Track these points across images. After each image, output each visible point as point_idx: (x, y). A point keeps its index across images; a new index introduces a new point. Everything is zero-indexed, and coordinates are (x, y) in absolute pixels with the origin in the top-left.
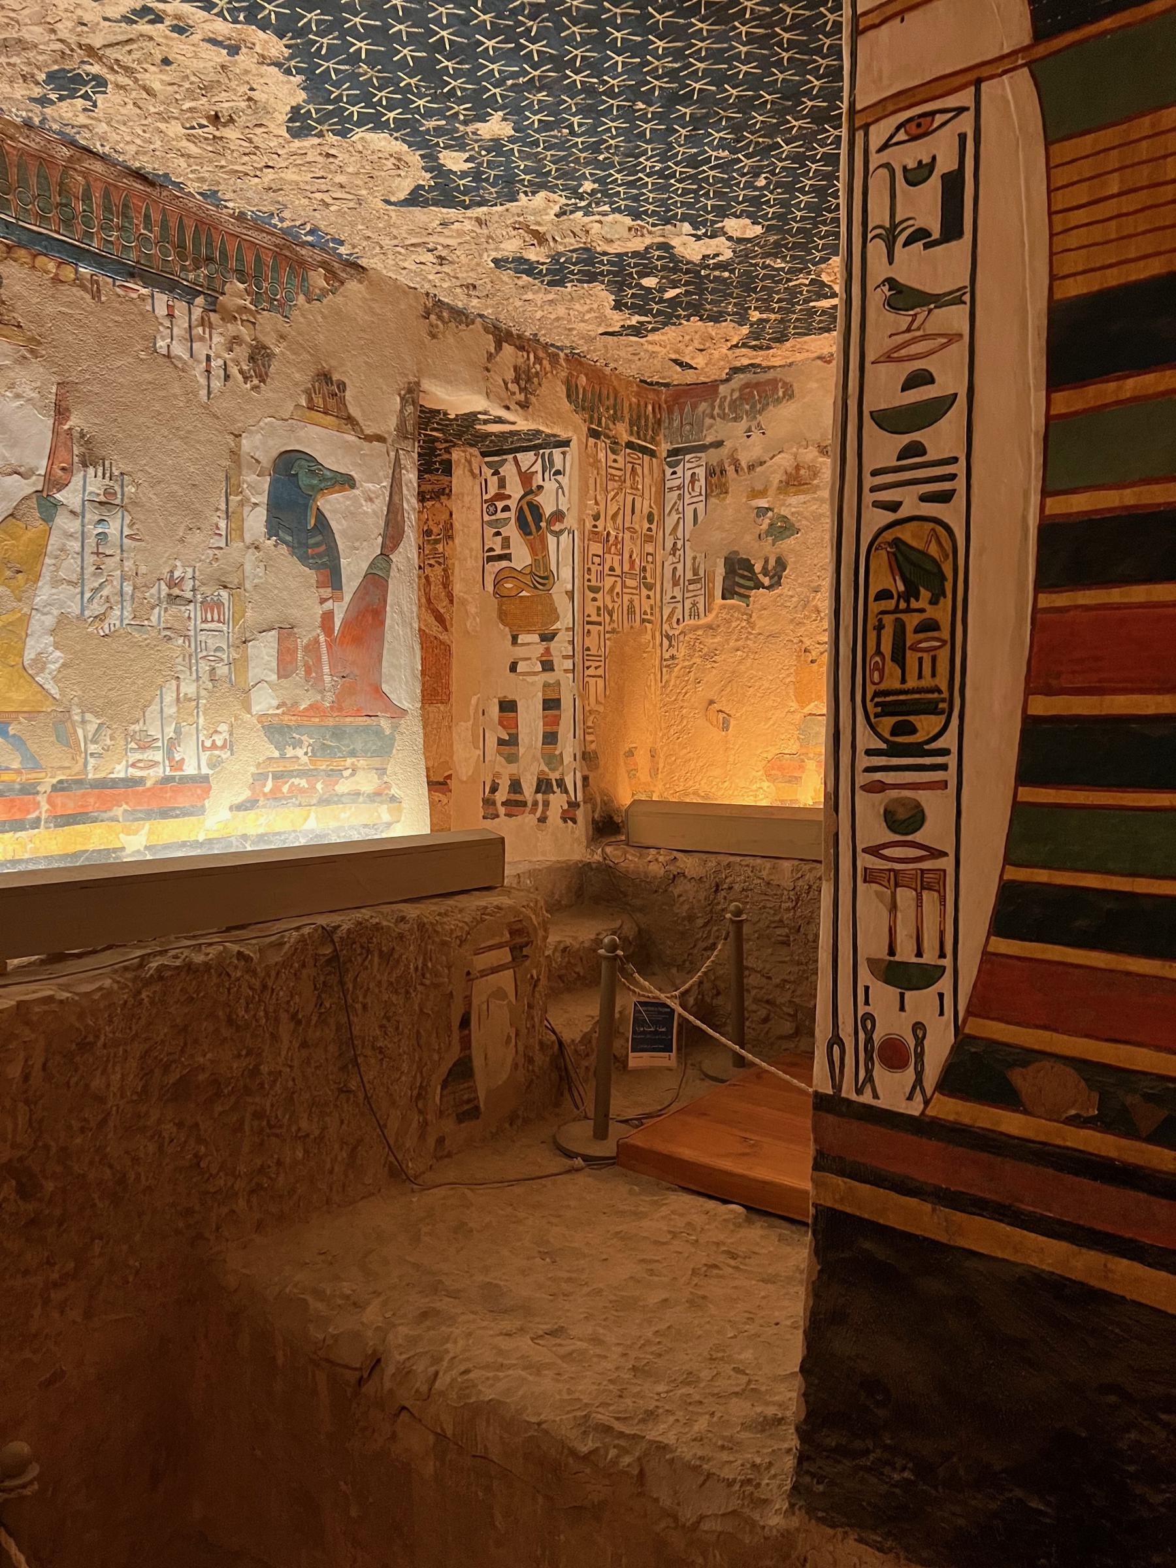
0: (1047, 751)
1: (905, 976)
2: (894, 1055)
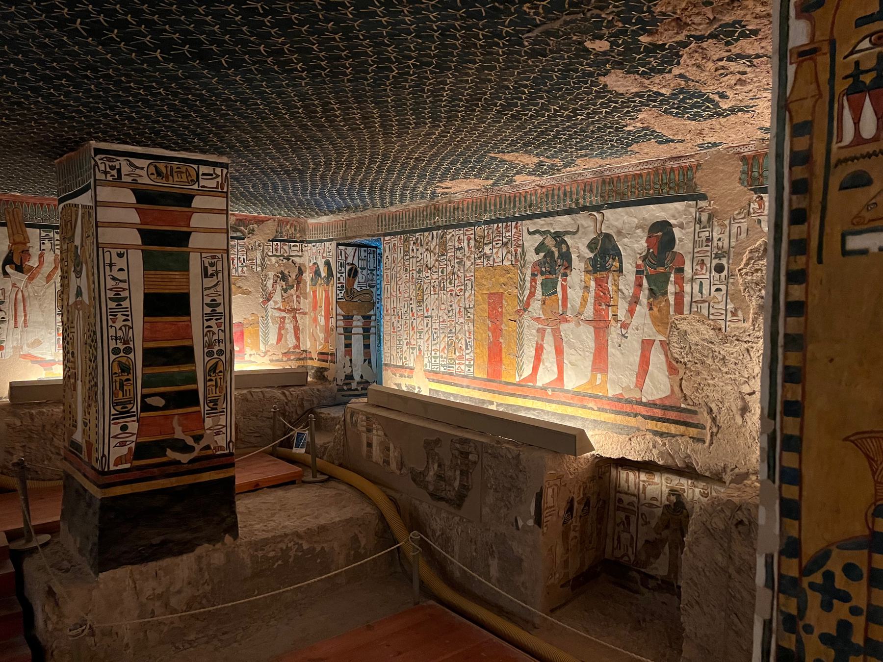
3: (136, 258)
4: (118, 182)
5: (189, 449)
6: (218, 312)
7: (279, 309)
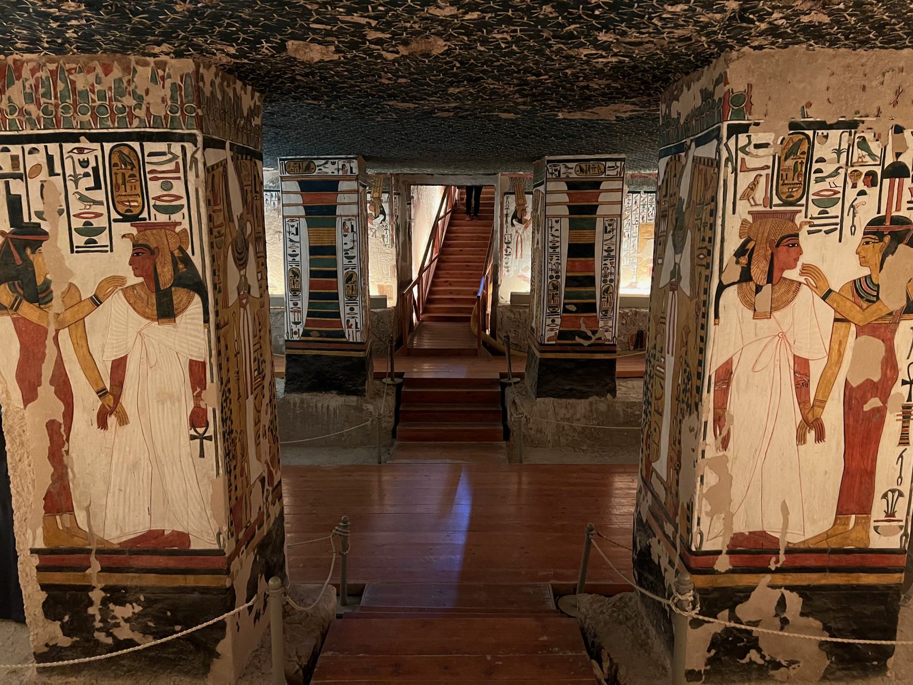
0: (312, 296)
1: (296, 323)
2: (295, 333)
3: (565, 222)
4: (558, 178)
5: (589, 338)
6: (612, 256)
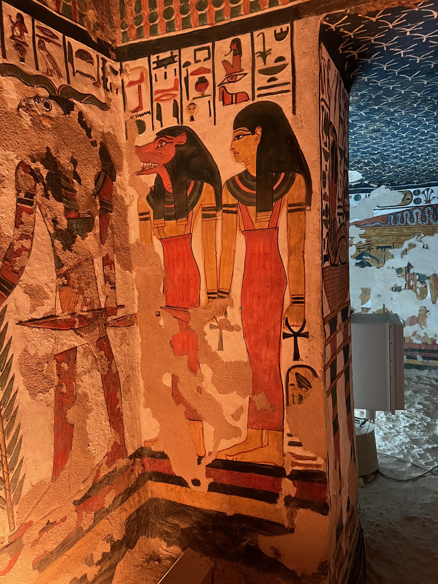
7: (50, 322)
